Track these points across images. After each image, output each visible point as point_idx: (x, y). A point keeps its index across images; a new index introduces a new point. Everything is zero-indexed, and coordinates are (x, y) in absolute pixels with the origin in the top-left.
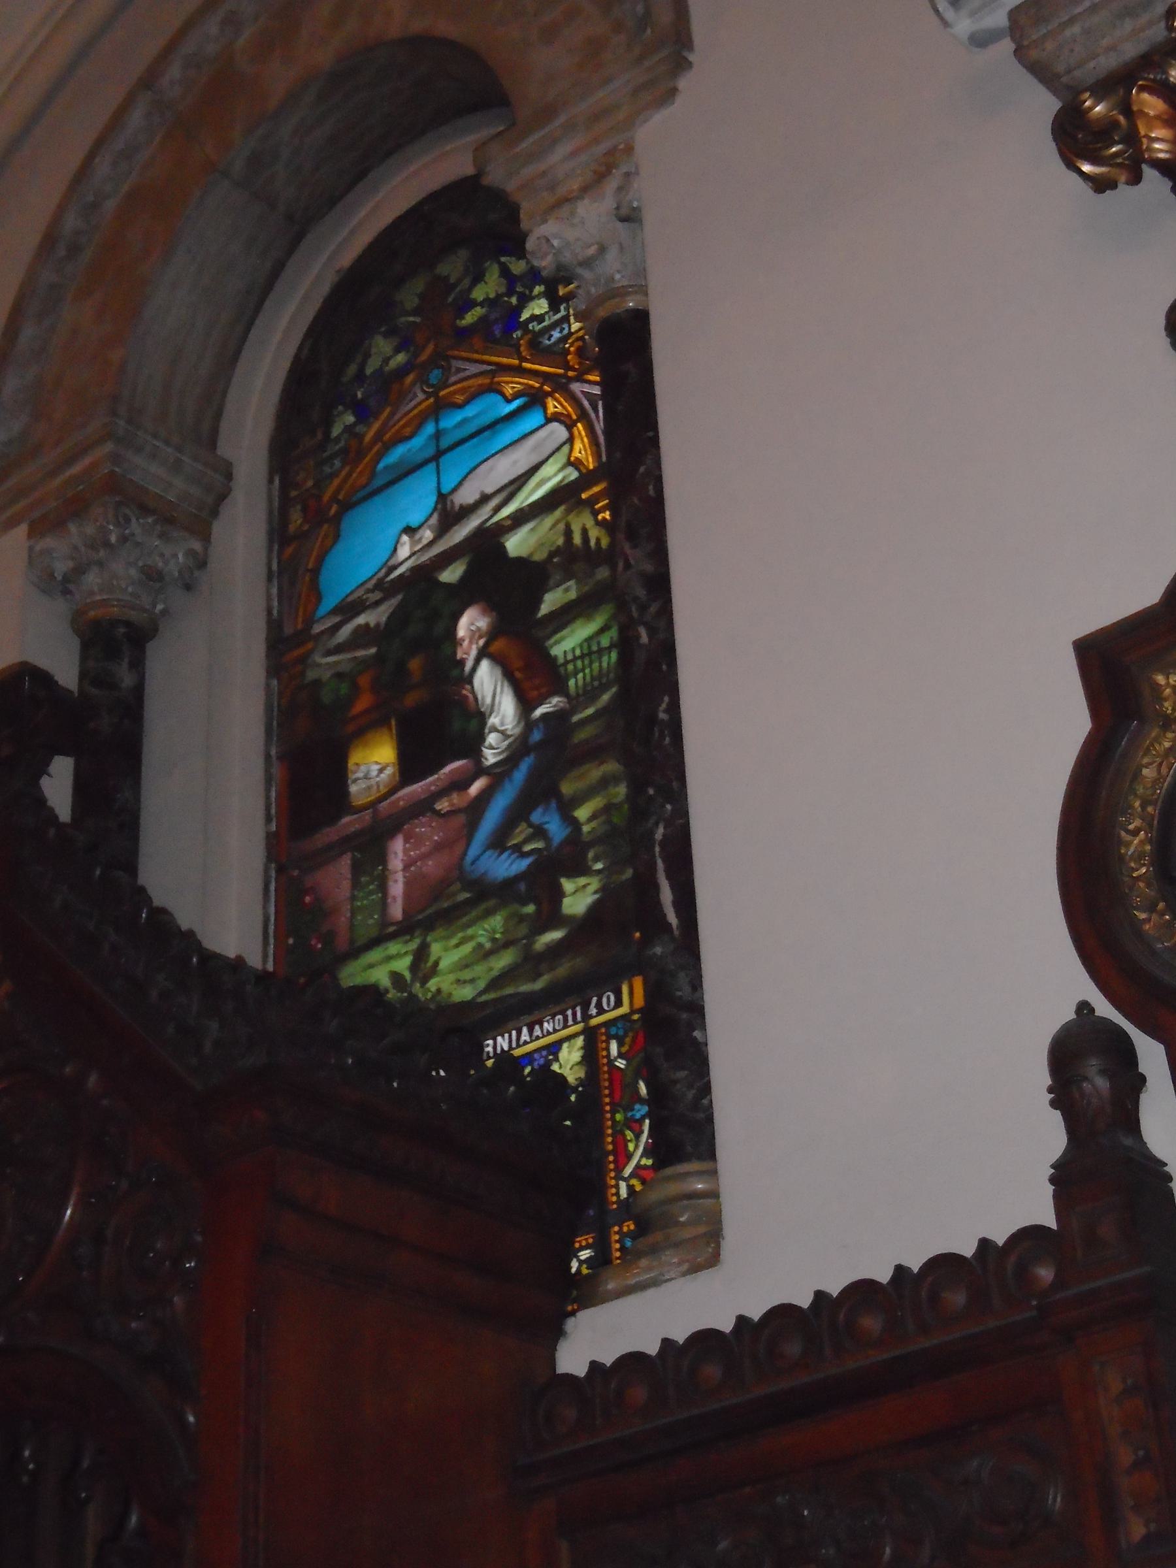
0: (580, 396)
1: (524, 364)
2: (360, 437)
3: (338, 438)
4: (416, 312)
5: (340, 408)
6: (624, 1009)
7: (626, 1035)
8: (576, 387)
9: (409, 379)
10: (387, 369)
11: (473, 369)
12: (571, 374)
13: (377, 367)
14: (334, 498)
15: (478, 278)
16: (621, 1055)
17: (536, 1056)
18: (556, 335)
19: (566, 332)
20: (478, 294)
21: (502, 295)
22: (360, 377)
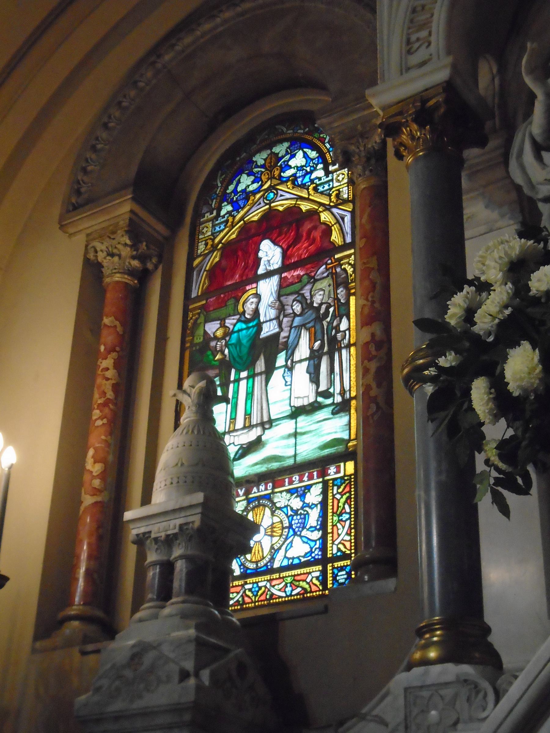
0: (337, 214)
1: (310, 197)
2: (234, 217)
3: (223, 217)
4: (263, 166)
5: (226, 203)
6: (342, 474)
7: (341, 485)
8: (335, 210)
9: (258, 196)
10: (248, 190)
11: (288, 196)
12: (332, 204)
13: (244, 188)
14: (220, 242)
15: (293, 156)
16: (338, 493)
17: (299, 489)
18: (326, 187)
19: (331, 186)
20: (292, 163)
22: (235, 191)
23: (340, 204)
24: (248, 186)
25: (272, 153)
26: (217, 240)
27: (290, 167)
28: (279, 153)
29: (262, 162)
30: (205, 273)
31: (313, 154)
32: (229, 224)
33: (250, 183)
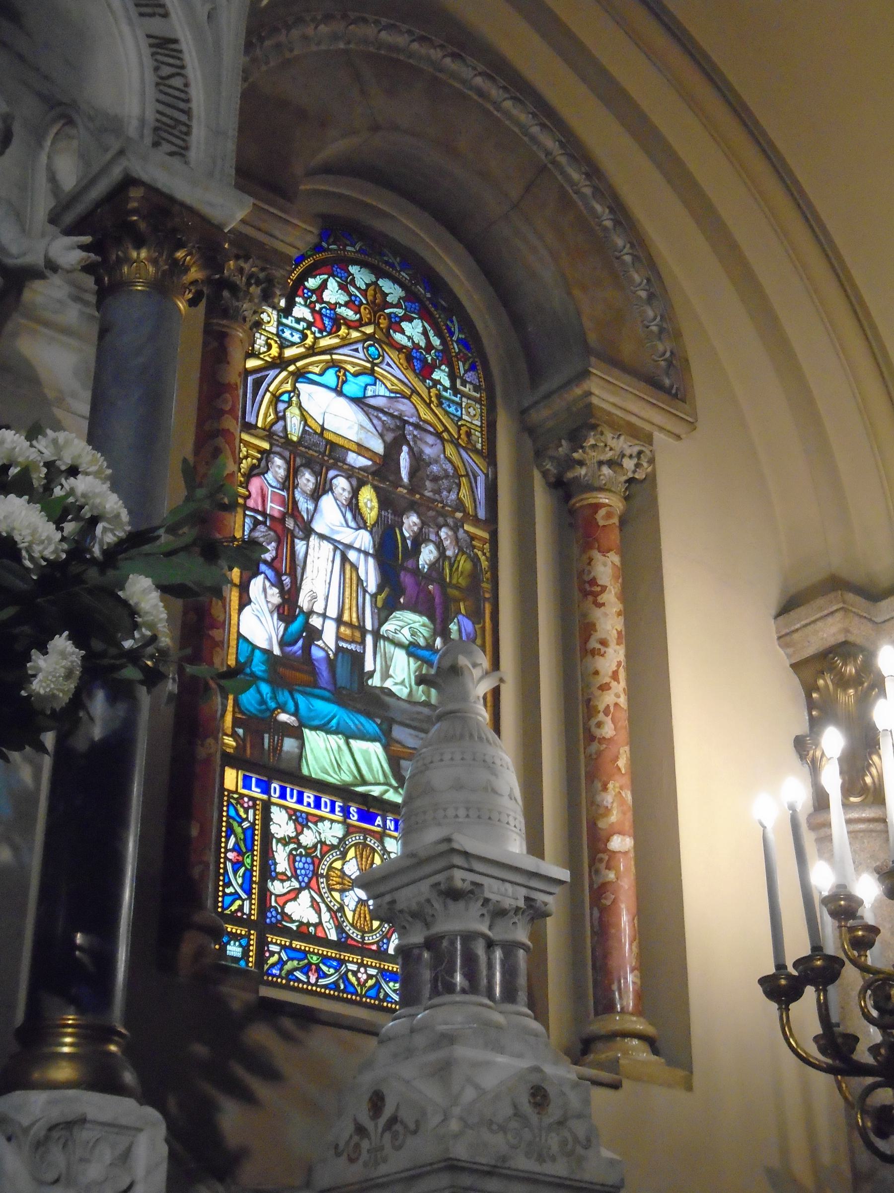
3: (298, 321)
21: (421, 348)
23: (472, 451)
24: (341, 305)
25: (375, 283)
26: (289, 353)
27: (402, 332)
28: (387, 295)
29: (363, 287)
30: (268, 395)
31: (436, 342)
32: (309, 341)
33: (342, 303)
